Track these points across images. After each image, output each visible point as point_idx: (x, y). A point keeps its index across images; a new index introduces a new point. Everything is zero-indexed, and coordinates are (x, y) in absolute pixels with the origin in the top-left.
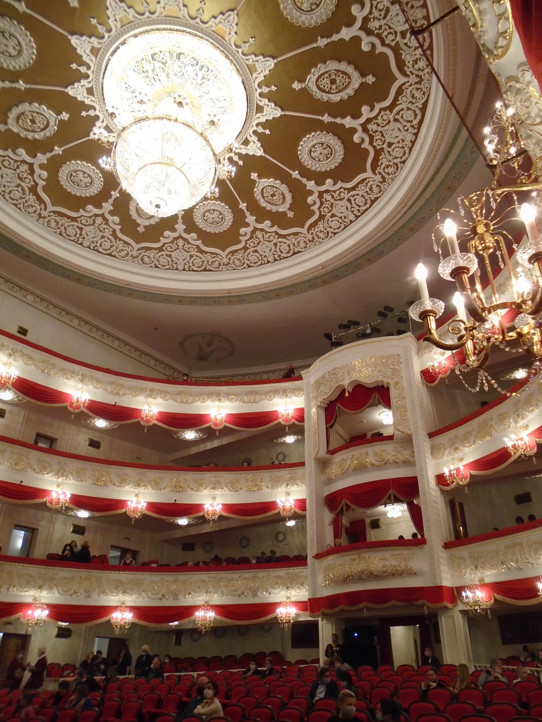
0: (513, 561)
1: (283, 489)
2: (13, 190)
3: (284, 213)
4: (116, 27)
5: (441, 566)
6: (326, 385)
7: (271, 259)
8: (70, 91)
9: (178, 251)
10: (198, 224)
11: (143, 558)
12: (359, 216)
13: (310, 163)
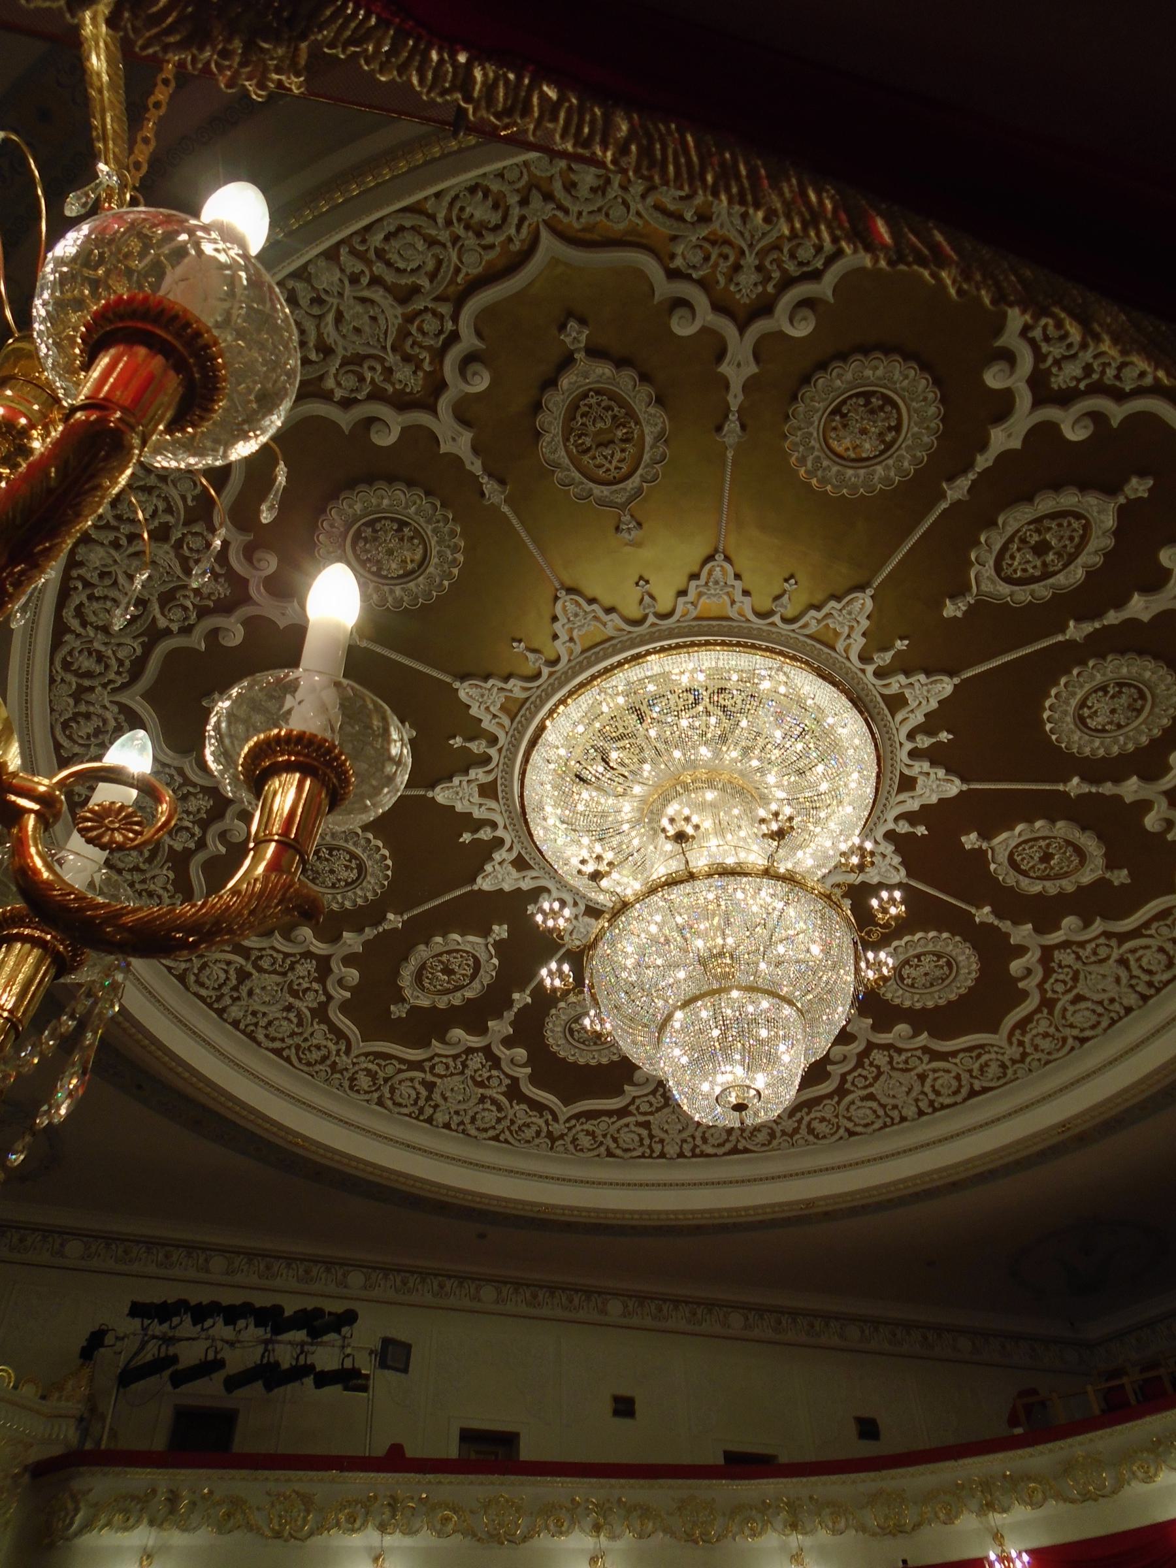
2: (476, 1113)
3: (1101, 884)
4: (502, 726)
7: (1131, 999)
8: (484, 884)
9: (883, 1078)
10: (897, 1001)
13: (1097, 743)
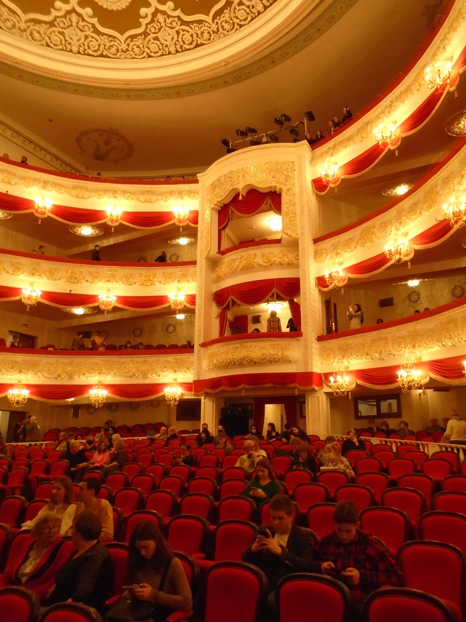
0: (377, 352)
5: (313, 355)
6: (221, 188)
7: (173, 49)
11: (40, 343)
12: (268, 7)
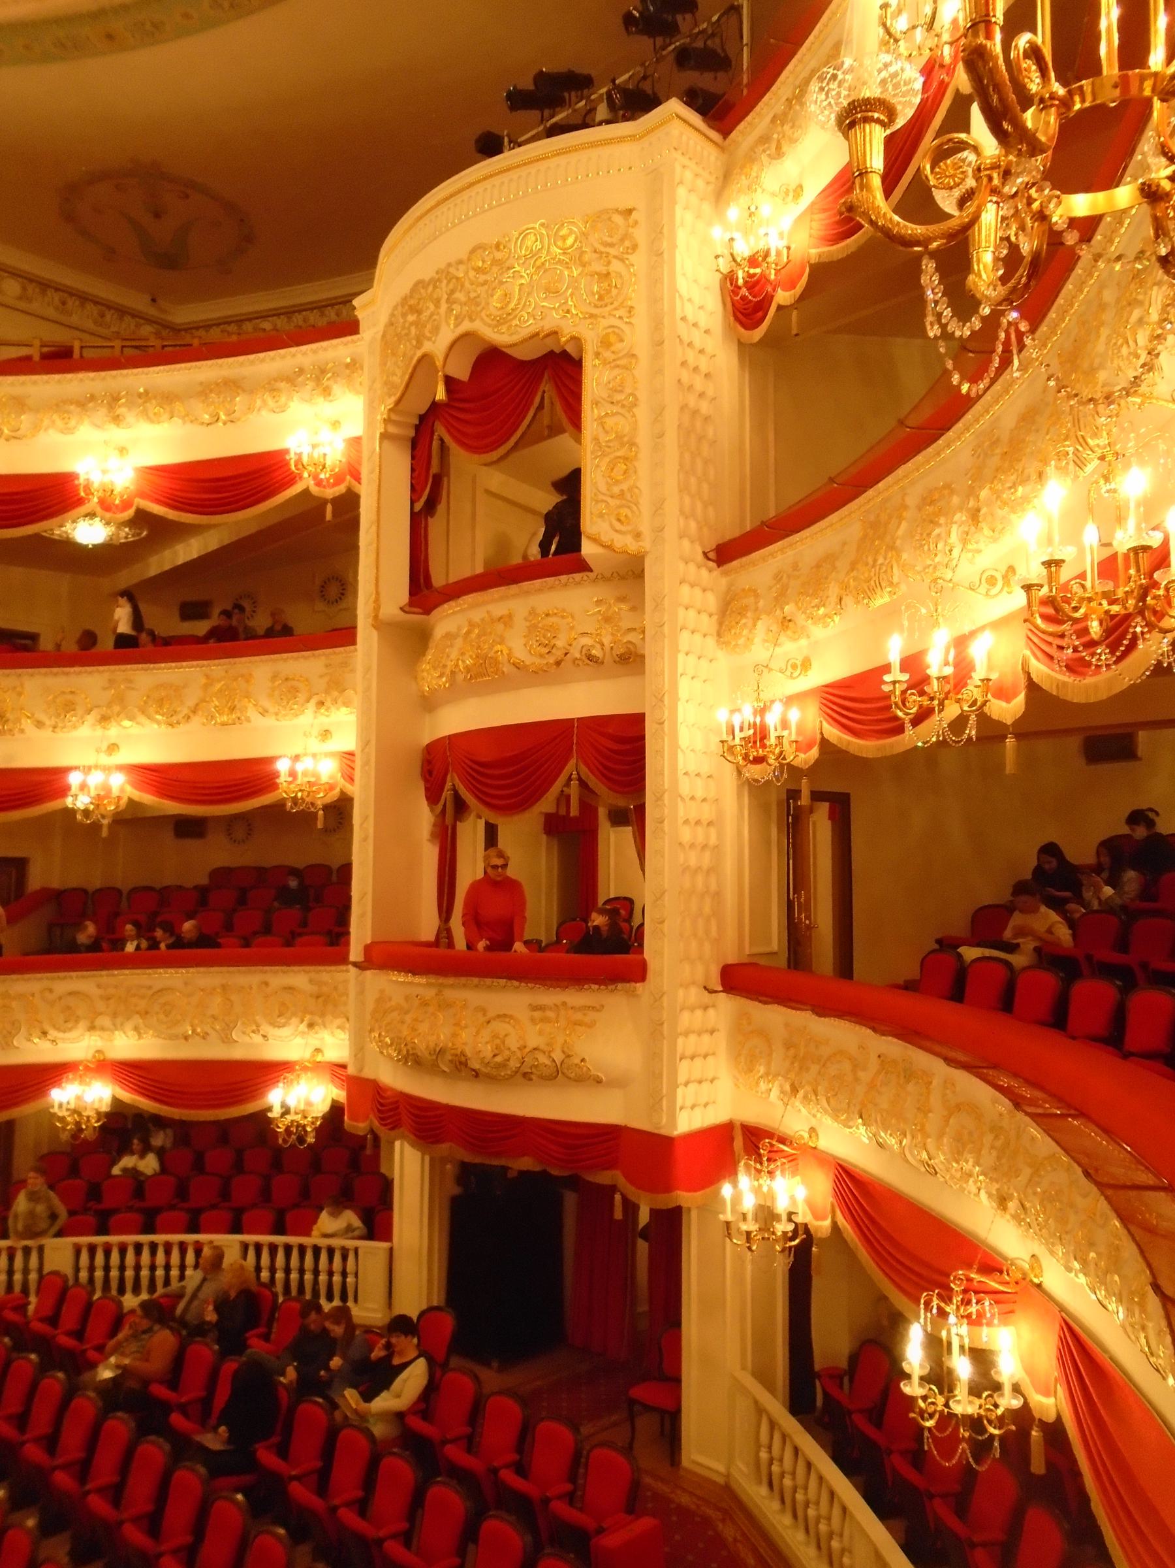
1: (308, 718)
